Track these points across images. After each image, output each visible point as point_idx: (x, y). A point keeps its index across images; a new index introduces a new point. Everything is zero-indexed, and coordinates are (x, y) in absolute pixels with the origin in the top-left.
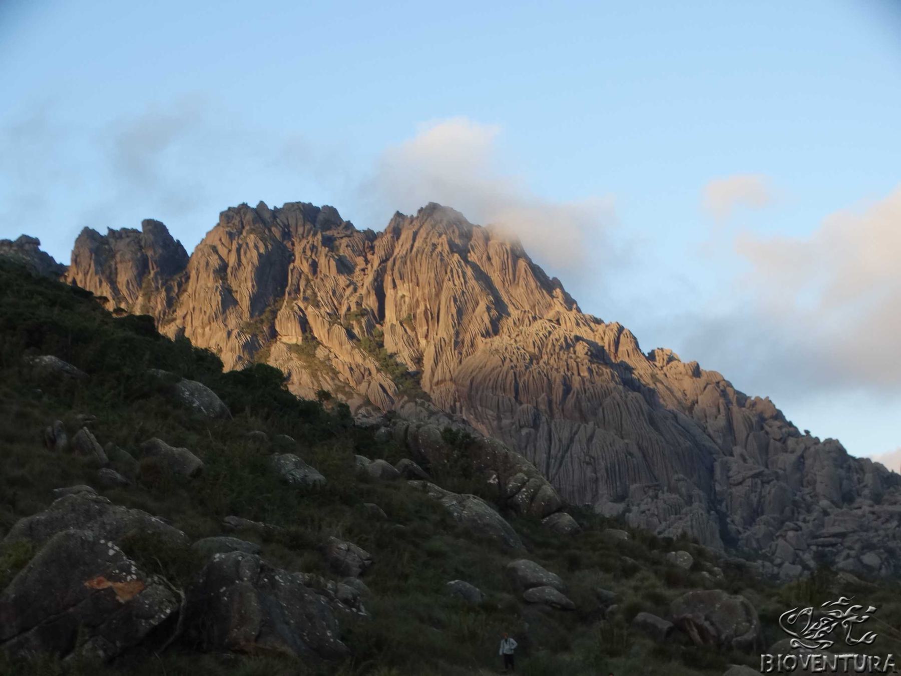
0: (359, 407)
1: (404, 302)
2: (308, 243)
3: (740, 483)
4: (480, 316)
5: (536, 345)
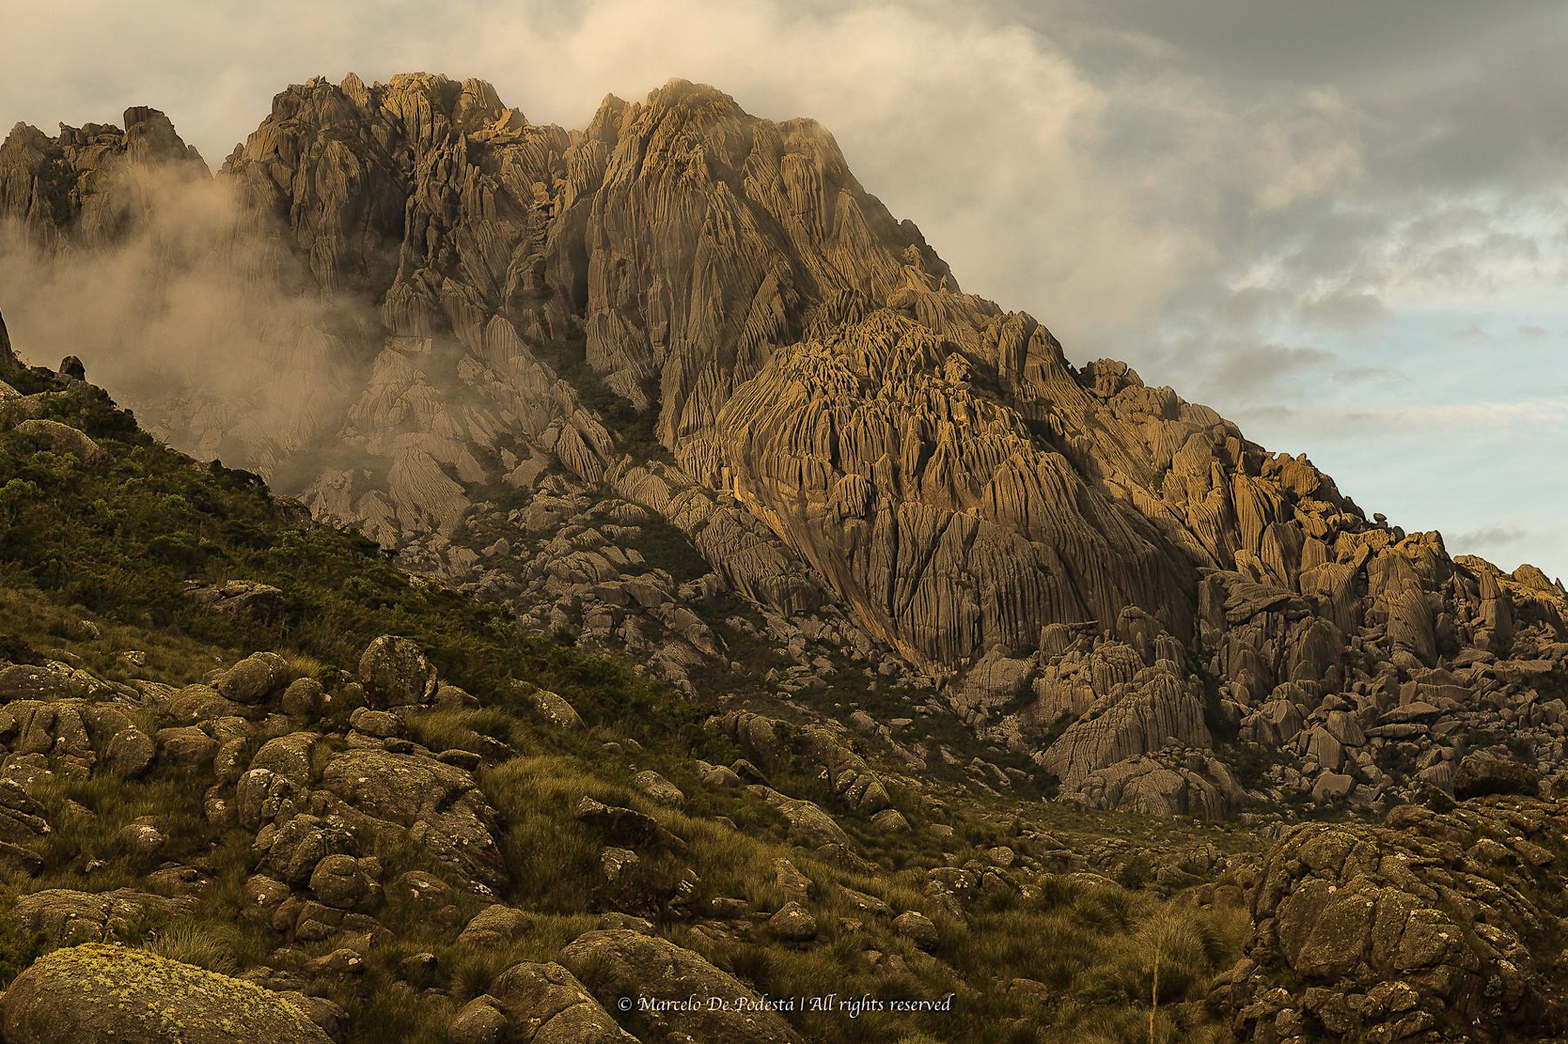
0: (541, 477)
2: (441, 156)
3: (1247, 621)
5: (871, 361)
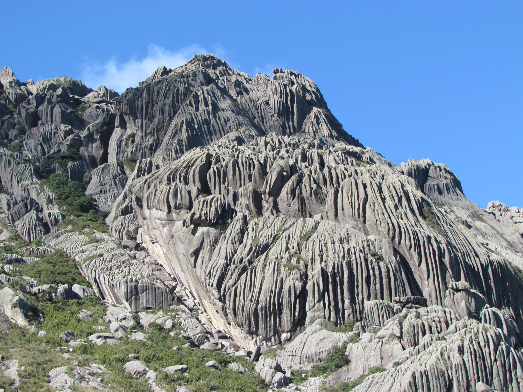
1: (133, 141)
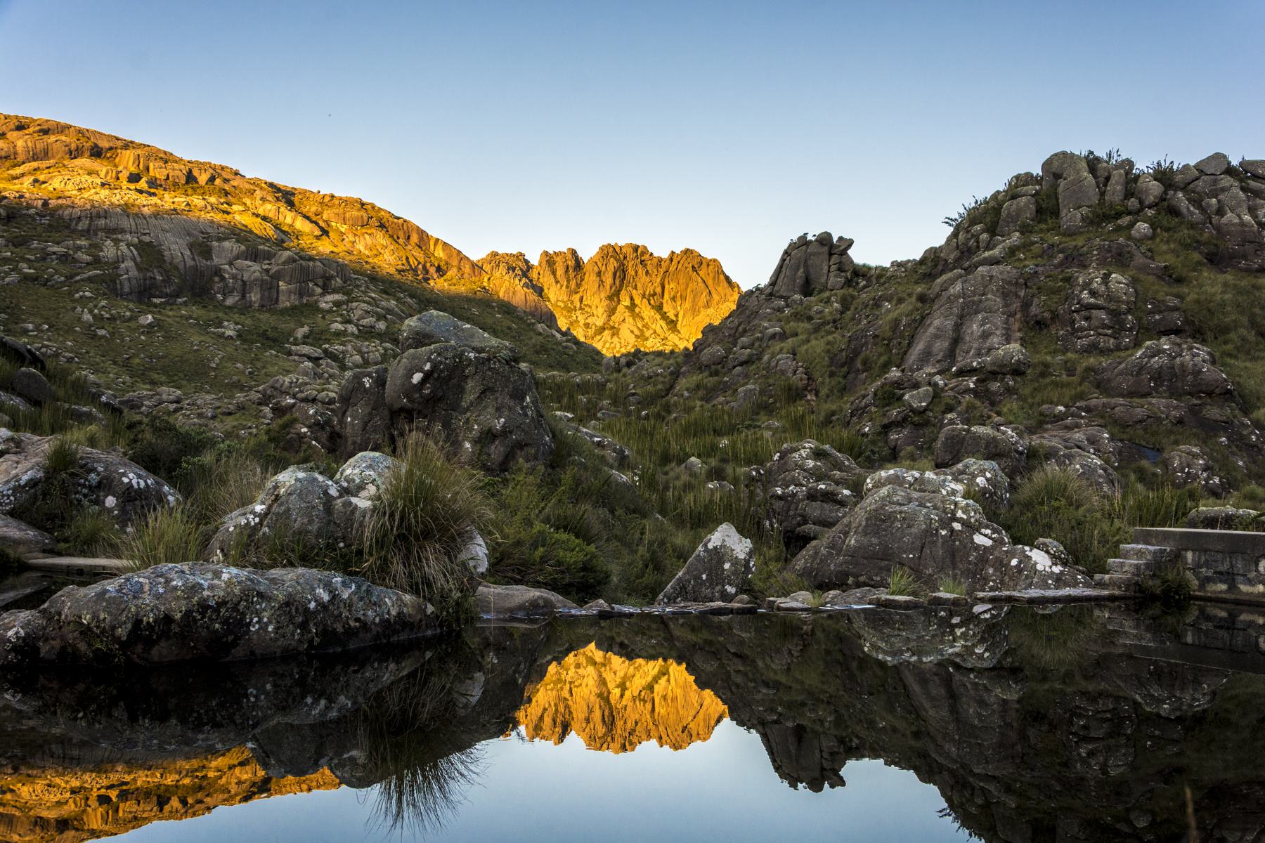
4: (703, 299)
